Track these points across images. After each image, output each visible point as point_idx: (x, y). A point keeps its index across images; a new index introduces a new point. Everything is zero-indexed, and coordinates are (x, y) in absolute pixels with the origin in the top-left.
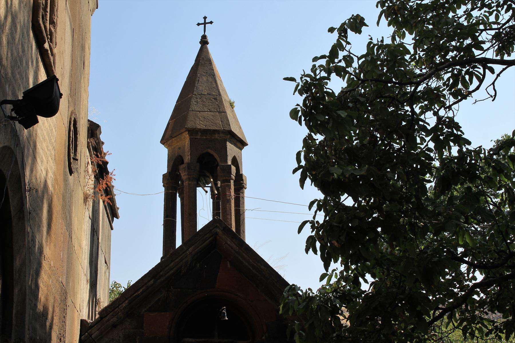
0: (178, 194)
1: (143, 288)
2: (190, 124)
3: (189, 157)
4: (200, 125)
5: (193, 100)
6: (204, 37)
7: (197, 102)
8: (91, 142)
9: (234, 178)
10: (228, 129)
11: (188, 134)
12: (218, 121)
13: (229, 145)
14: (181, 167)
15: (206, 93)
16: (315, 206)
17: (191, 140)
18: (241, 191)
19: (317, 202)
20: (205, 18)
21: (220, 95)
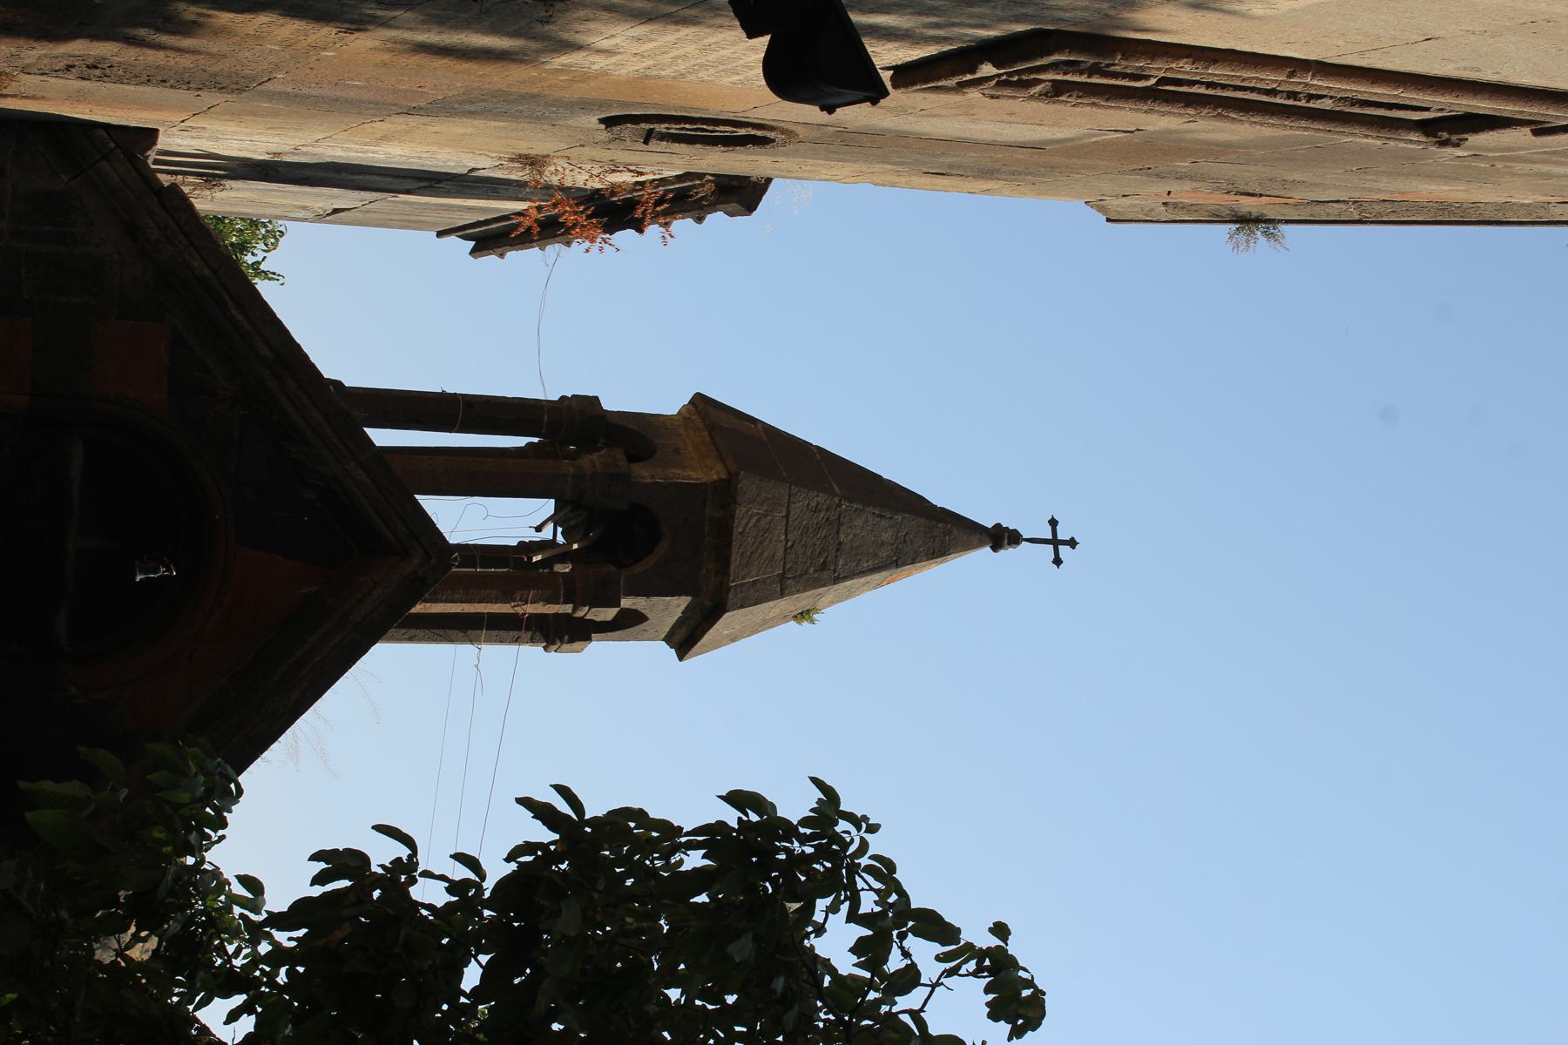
0: (536, 440)
2: (748, 485)
3: (649, 480)
4: (746, 517)
5: (820, 498)
6: (1014, 538)
7: (817, 510)
8: (702, 185)
9: (580, 614)
10: (730, 602)
11: (720, 480)
14: (619, 455)
16: (461, 873)
17: (701, 487)
18: (538, 636)
19: (472, 876)
20: (1072, 543)
21: (836, 580)
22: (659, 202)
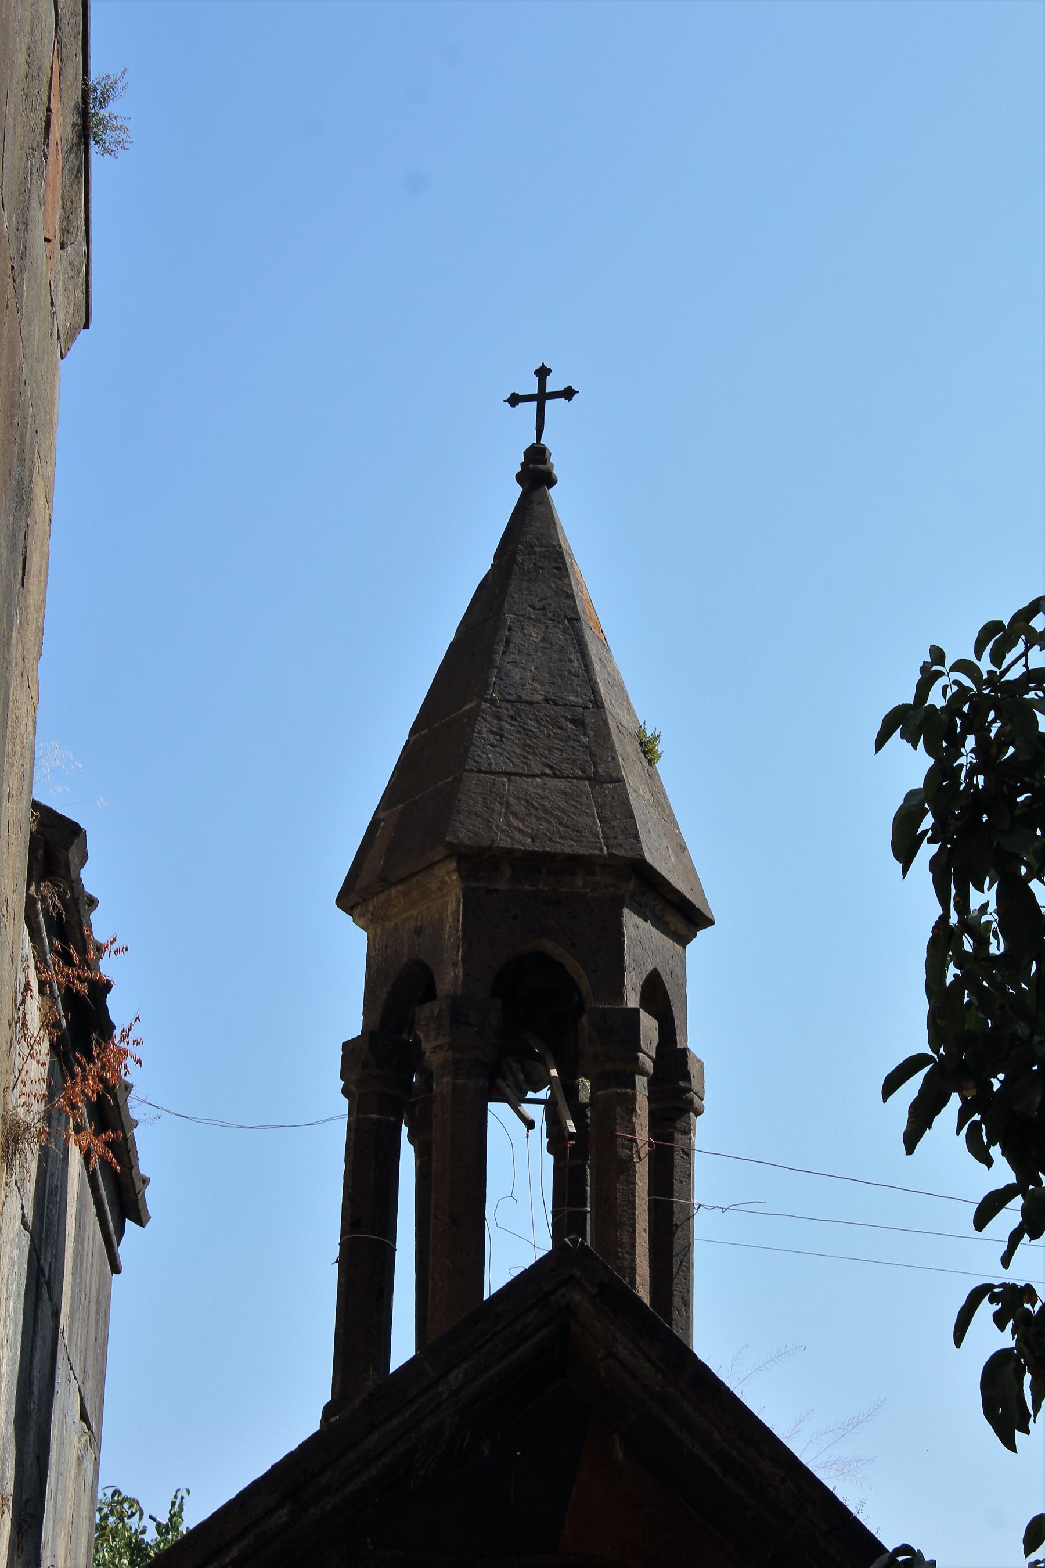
0: (405, 1130)
1: (245, 1542)
2: (466, 830)
3: (460, 971)
4: (511, 832)
5: (483, 727)
6: (536, 455)
7: (499, 734)
8: (44, 899)
9: (649, 1065)
10: (630, 854)
11: (459, 870)
12: (588, 820)
13: (630, 920)
14: (425, 1012)
15: (538, 697)
17: (470, 899)
18: (680, 1124)
20: (543, 373)
21: (598, 704)
22: (68, 960)
